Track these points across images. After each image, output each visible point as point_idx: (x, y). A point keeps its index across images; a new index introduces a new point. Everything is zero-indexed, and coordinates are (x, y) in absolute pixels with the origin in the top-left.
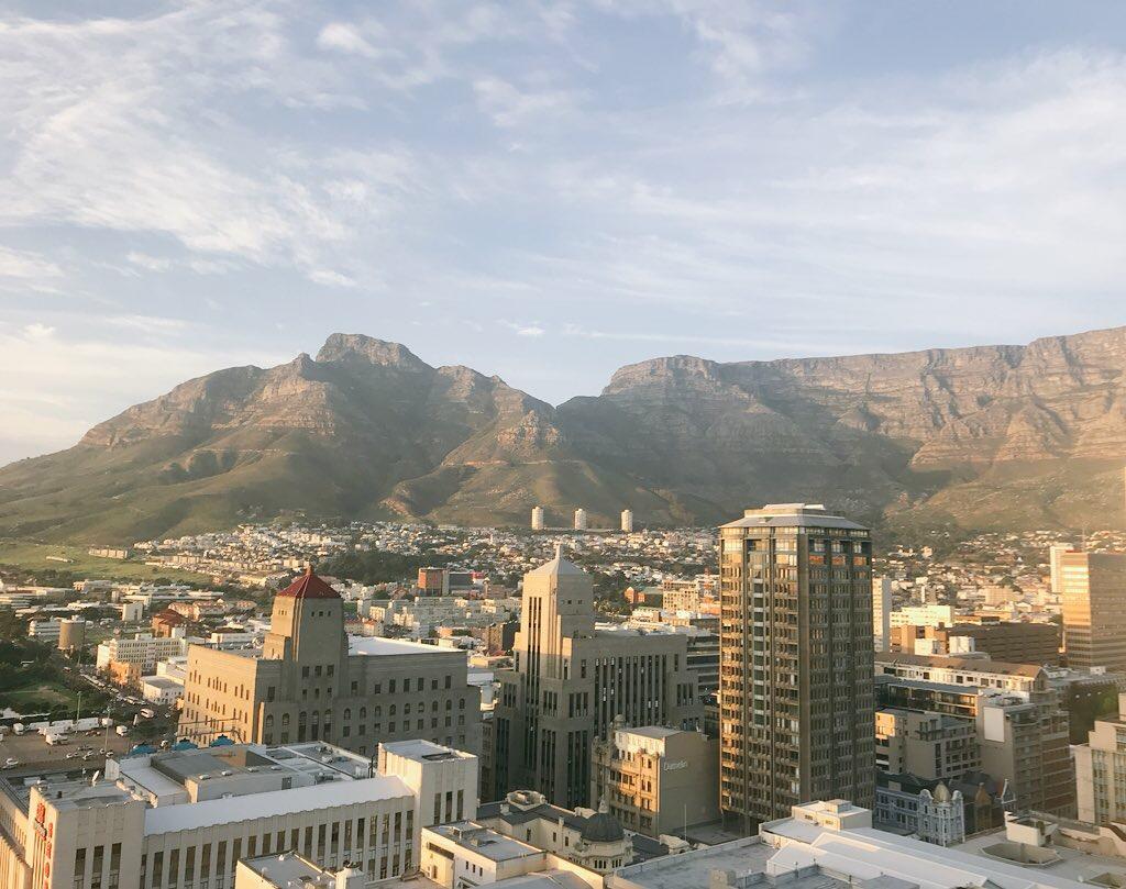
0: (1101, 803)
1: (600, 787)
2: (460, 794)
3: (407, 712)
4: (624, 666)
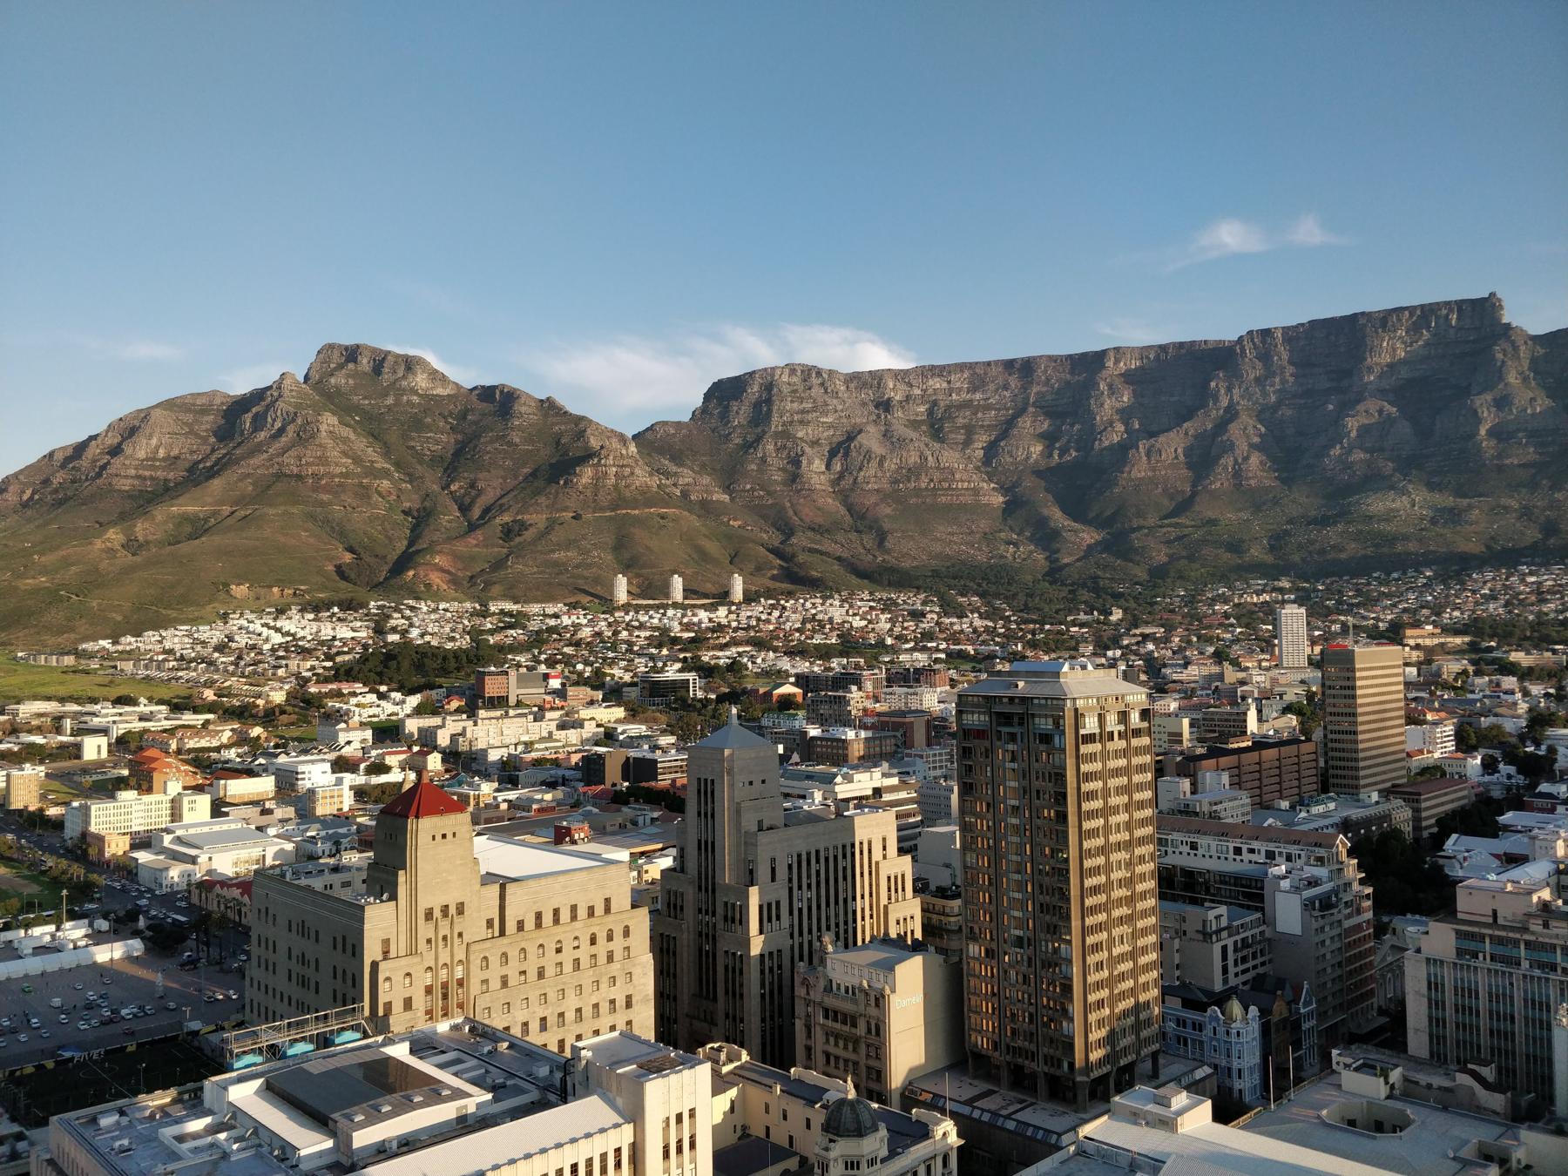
0: (1436, 1022)
1: (808, 1028)
2: (692, 1113)
3: (559, 951)
4: (822, 861)
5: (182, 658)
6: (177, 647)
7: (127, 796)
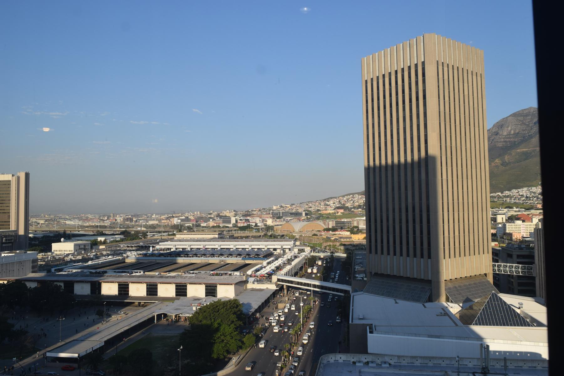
5: (527, 197)
6: (525, 195)
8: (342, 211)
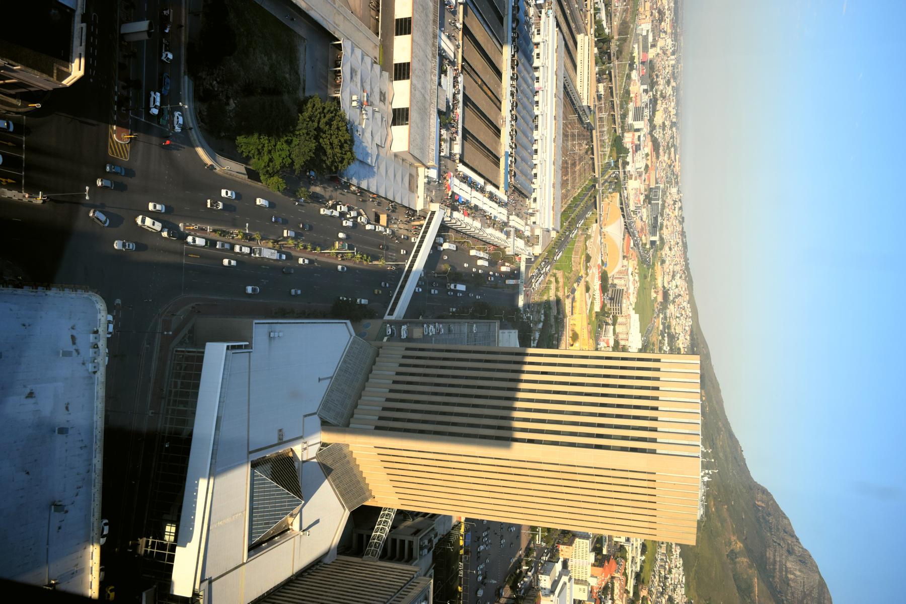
5: (666, 578)
6: (672, 576)
7: (592, 557)
8: (660, 299)
